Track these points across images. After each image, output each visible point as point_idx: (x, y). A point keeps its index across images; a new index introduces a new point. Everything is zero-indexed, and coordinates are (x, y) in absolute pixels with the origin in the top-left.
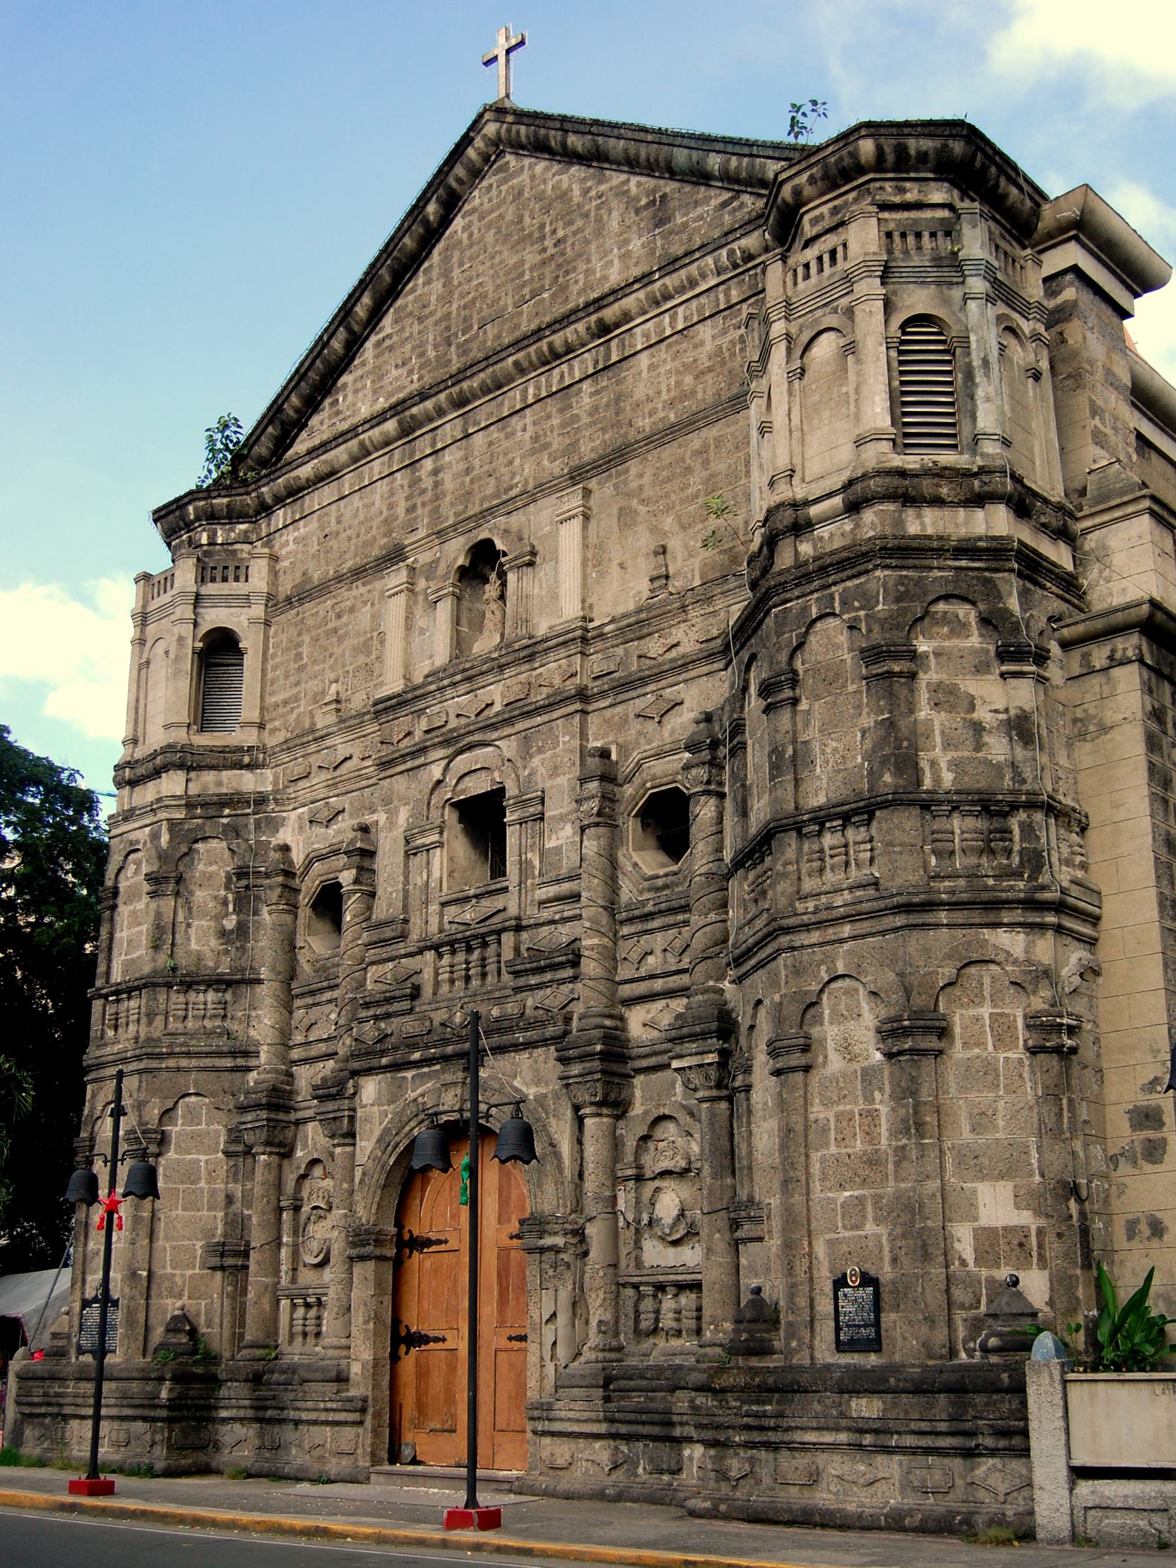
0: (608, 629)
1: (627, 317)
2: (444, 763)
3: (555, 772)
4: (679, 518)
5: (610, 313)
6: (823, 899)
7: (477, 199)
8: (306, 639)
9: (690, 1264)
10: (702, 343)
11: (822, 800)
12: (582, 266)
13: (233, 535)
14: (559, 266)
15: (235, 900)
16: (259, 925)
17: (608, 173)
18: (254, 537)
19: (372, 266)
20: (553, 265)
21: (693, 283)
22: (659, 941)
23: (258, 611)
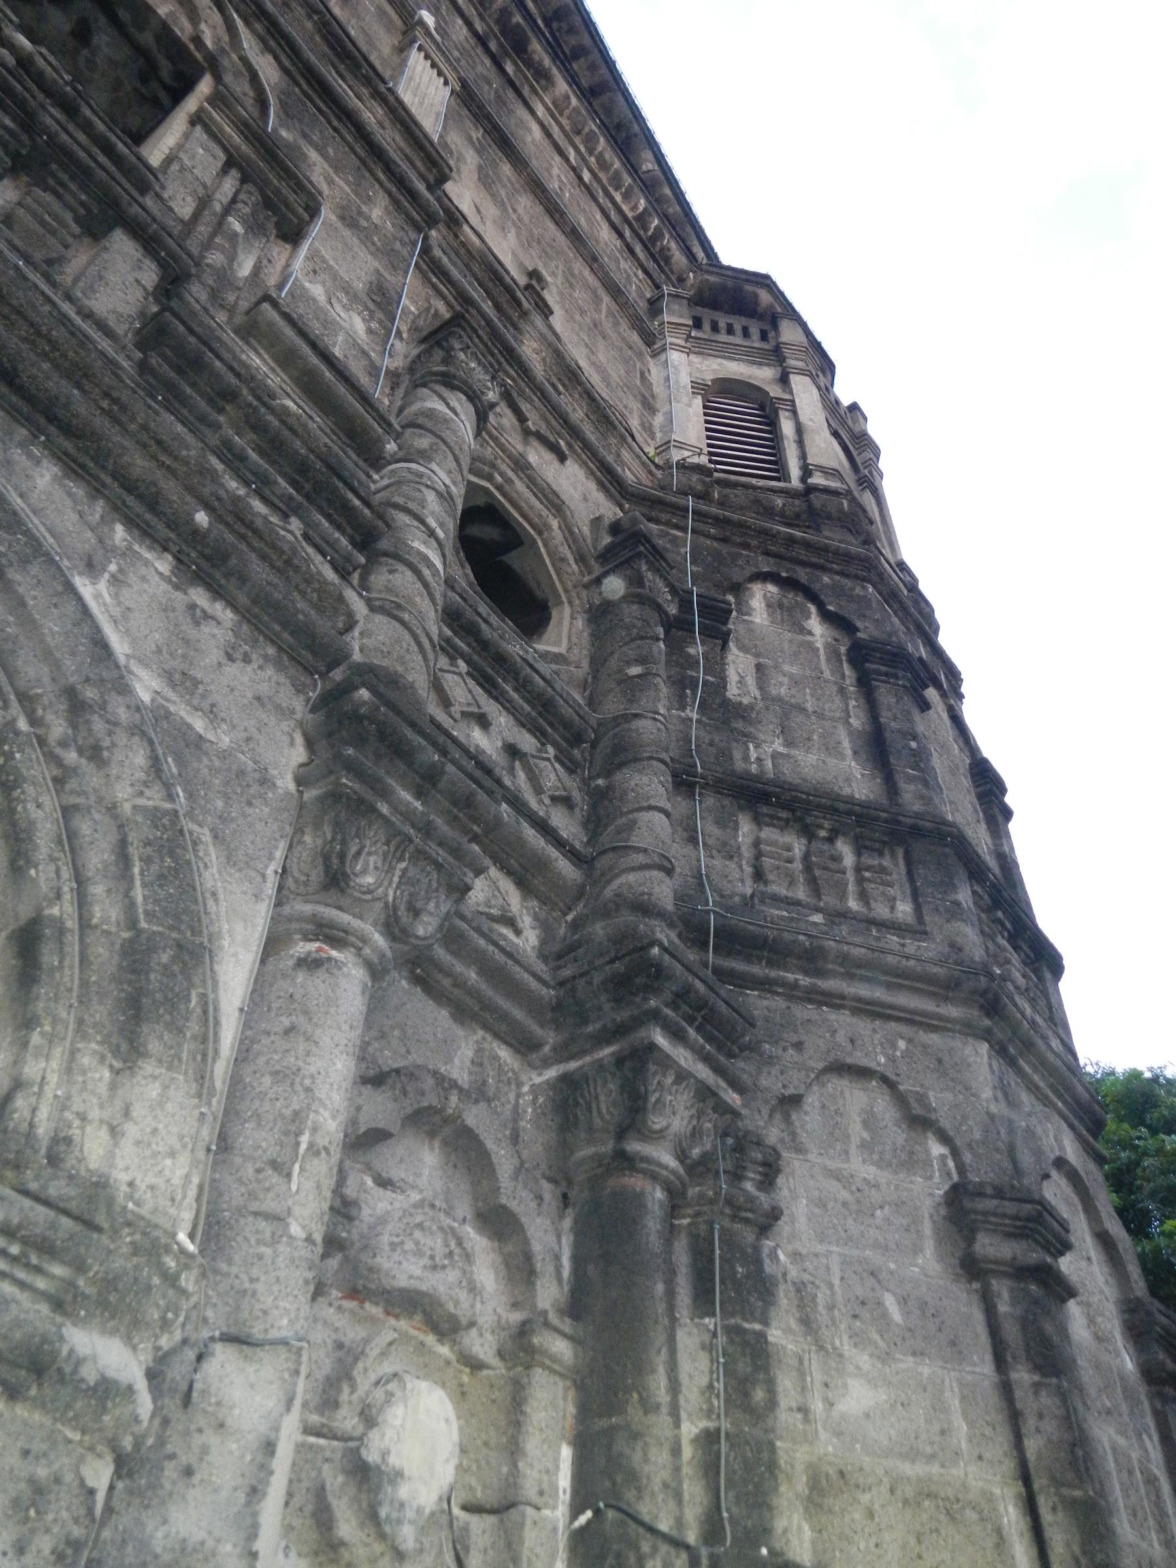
21: (616, 182)
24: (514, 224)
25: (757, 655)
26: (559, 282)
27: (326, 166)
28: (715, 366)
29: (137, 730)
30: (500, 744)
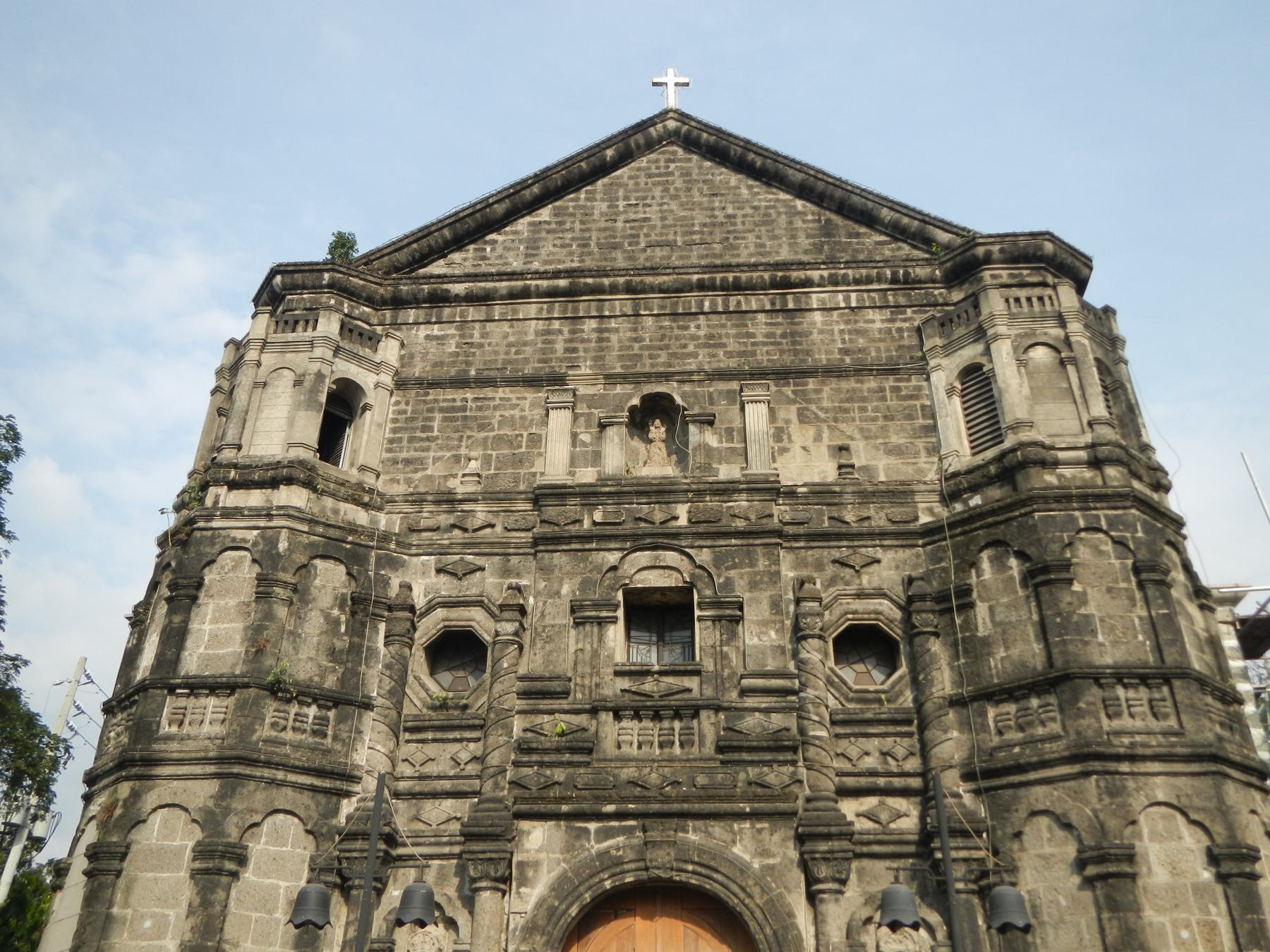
0: (800, 490)
1: (808, 283)
2: (618, 555)
3: (753, 585)
4: (861, 430)
5: (795, 275)
6: (1138, 738)
7: (643, 162)
8: (438, 416)
10: (873, 321)
11: (1108, 660)
12: (751, 238)
13: (357, 312)
14: (729, 232)
15: (347, 621)
16: (372, 652)
17: (774, 190)
18: (375, 321)
19: (548, 169)
20: (725, 229)
21: (869, 280)
23: (387, 379)
24: (825, 421)
25: (988, 600)
26: (858, 422)
27: (738, 571)
28: (958, 360)
29: (756, 884)
30: (877, 754)
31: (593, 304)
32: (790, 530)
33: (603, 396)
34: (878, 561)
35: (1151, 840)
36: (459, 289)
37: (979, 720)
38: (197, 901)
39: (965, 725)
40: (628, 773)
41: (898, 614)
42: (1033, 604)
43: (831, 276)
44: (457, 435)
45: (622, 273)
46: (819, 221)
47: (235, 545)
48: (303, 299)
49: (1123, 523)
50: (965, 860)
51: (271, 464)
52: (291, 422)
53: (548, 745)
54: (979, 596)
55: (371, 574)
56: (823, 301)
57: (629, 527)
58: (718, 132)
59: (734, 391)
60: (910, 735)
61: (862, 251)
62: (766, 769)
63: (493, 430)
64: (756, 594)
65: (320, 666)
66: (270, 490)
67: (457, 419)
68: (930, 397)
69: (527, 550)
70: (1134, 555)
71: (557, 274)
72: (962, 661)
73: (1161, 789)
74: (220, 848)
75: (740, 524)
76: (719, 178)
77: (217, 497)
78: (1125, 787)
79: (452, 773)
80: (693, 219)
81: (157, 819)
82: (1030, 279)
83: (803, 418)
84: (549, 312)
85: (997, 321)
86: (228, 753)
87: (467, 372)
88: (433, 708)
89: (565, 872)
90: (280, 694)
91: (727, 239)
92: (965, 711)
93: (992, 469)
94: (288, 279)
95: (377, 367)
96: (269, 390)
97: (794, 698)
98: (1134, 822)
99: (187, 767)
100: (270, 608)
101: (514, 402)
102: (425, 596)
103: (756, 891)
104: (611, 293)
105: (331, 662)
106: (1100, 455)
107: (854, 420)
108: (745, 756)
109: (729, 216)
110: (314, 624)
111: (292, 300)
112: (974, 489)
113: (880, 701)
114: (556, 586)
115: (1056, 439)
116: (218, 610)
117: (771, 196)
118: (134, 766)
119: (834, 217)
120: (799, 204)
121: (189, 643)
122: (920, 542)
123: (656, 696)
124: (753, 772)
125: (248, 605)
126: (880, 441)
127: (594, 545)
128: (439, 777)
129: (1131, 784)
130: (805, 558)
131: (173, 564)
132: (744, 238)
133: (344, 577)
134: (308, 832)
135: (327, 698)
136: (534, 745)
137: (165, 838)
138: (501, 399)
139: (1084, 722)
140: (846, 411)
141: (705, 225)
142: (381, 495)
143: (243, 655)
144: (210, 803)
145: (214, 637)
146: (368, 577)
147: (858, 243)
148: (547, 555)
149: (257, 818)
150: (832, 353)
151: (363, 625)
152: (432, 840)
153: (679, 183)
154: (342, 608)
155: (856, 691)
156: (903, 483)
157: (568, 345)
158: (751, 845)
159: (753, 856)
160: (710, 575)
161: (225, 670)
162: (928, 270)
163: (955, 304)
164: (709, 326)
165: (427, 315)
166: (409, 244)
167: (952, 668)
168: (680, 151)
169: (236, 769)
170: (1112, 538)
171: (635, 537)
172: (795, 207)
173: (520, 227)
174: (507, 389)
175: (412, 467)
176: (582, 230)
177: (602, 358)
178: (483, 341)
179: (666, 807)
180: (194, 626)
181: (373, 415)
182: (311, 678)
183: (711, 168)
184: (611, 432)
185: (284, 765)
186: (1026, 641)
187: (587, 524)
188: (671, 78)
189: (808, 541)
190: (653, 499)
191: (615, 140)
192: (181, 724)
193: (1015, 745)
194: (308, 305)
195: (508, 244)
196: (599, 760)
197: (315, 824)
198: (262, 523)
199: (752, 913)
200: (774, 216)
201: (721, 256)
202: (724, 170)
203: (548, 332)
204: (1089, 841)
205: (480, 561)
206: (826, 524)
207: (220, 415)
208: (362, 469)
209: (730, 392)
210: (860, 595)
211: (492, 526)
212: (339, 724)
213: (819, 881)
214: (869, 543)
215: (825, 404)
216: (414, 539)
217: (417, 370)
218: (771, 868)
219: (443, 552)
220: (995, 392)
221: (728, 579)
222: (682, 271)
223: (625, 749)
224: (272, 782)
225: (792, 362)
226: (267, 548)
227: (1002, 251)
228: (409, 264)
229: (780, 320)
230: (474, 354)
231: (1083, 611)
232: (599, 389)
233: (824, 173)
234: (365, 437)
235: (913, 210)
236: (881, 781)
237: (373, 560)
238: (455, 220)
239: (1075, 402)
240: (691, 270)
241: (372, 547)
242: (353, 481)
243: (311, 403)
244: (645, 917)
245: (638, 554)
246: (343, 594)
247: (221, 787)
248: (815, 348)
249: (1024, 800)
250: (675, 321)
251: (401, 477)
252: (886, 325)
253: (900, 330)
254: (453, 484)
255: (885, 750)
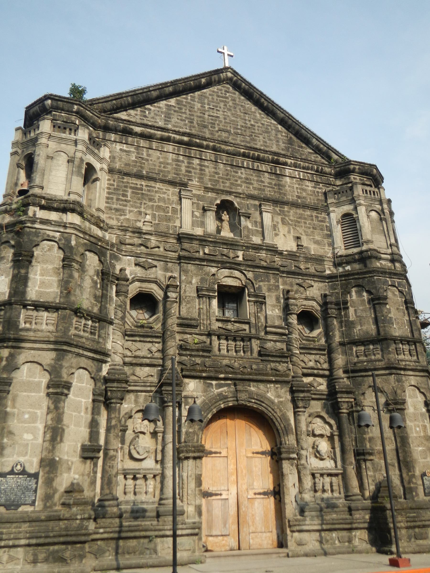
1: (285, 164)
3: (269, 290)
4: (305, 231)
5: (282, 159)
6: (407, 363)
7: (215, 88)
9: (329, 467)
11: (397, 334)
14: (252, 132)
15: (100, 283)
16: (111, 298)
21: (308, 169)
22: (312, 357)
23: (105, 167)
24: (291, 225)
25: (354, 307)
28: (342, 210)
31: (197, 152)
32: (282, 269)
33: (203, 196)
34: (312, 286)
35: (409, 398)
36: (138, 129)
37: (350, 351)
38: (52, 407)
39: (345, 353)
40: (226, 362)
41: (319, 308)
42: (372, 311)
43: (295, 163)
44: (139, 201)
45: (212, 141)
46: (287, 137)
47: (49, 238)
48: (62, 116)
49: (402, 285)
50: (347, 402)
51: (62, 200)
52: (69, 181)
53: (194, 348)
54: (351, 305)
55: (108, 261)
56: (290, 173)
57: (219, 258)
58: (249, 84)
59: (257, 205)
60: (324, 355)
61: (304, 155)
62: (277, 364)
63: (155, 202)
64: (270, 294)
65: (91, 303)
66: (61, 214)
67: (139, 194)
68: (330, 222)
69: (176, 261)
70: (405, 298)
71: (184, 134)
72: (344, 329)
73: (413, 380)
74: (63, 383)
75: (265, 264)
76: (247, 106)
77: (35, 212)
78: (402, 379)
79: (149, 356)
80: (237, 122)
81: (25, 368)
82: (367, 183)
83: (284, 222)
84: (178, 151)
85: (361, 198)
86: (60, 340)
87: (141, 171)
88: (137, 327)
89: (204, 401)
90: (78, 314)
91: (252, 135)
92: (344, 348)
93: (357, 257)
94: (55, 103)
95: (101, 160)
96: (55, 161)
97: (285, 337)
98: (404, 392)
99: (38, 344)
100: (71, 272)
101: (164, 191)
102: (130, 275)
103: (278, 411)
104: (206, 149)
105: (95, 301)
106: (395, 258)
107: (302, 227)
108: (270, 359)
109: (252, 125)
110: (87, 283)
111: (56, 115)
112: (348, 263)
113: (314, 341)
114: (190, 279)
115: (381, 249)
116: (43, 269)
117: (268, 120)
118: (10, 341)
119: (293, 137)
120: (280, 127)
121: (30, 284)
122: (327, 281)
123: (233, 331)
124: (273, 365)
125: (59, 269)
126: (311, 237)
127: (205, 263)
128: (143, 357)
129: (404, 378)
130: (286, 281)
131: (13, 243)
132: (258, 137)
133: (98, 262)
134: (92, 378)
135: (96, 318)
136: (188, 347)
137: (31, 377)
138: (158, 188)
139: (392, 355)
140: (299, 222)
141: (242, 126)
142: (107, 224)
143: (59, 293)
144: (53, 362)
145: (43, 283)
146: (107, 263)
147: (302, 151)
148: (185, 265)
149: (73, 370)
150: (294, 197)
151: (107, 285)
152: (143, 384)
153: (231, 103)
154: (98, 276)
155: (306, 337)
156: (321, 256)
157: (187, 169)
158: (274, 393)
159: (275, 398)
160: (252, 283)
161: (50, 299)
162: (330, 169)
163: (337, 186)
164: (246, 174)
165: (120, 138)
166: (112, 100)
167: (339, 331)
168: (231, 88)
169: (65, 348)
170: (399, 290)
171: (222, 262)
172: (278, 128)
173: (161, 105)
174: (161, 184)
175: (118, 213)
176: (189, 114)
177: (202, 178)
178: (148, 158)
179: (244, 377)
180: (31, 276)
181: (101, 184)
182: (88, 308)
183: (244, 100)
184: (209, 213)
185: (82, 347)
186: (369, 324)
187: (201, 253)
188: (226, 52)
189: (287, 274)
190: (229, 247)
191: (206, 75)
192: (31, 323)
193: (365, 362)
194: (65, 120)
195: (156, 112)
196: (214, 356)
197: (95, 375)
198: (62, 230)
199: (276, 419)
200: (270, 130)
201: (249, 143)
202: (249, 102)
203: (178, 161)
204: (391, 397)
205: (155, 263)
206: (293, 268)
207: (18, 167)
208: (98, 210)
209: (255, 205)
210: (306, 299)
211: (159, 247)
212: (102, 329)
213: (298, 407)
214: (309, 278)
215: (291, 218)
216: (124, 248)
217: (117, 165)
218: (281, 402)
219: (137, 256)
220: (358, 227)
221: (259, 286)
222: (237, 146)
223: (222, 352)
224: (79, 355)
225: (279, 197)
226: (66, 243)
227: (359, 169)
228: (110, 110)
229: (274, 177)
230: (144, 163)
231: (389, 316)
232: (201, 193)
233: (292, 117)
234: (98, 194)
235: (325, 142)
236: (316, 371)
237: (108, 255)
238: (134, 94)
239: (385, 236)
240: (241, 147)
241: (108, 249)
242: (96, 215)
243: (79, 173)
244: (230, 419)
245: (223, 270)
246: (98, 270)
247: (57, 355)
248: (287, 193)
249: (367, 382)
250: (232, 168)
251: (114, 216)
252: (313, 189)
253: (318, 192)
254: (140, 224)
255: (317, 360)
